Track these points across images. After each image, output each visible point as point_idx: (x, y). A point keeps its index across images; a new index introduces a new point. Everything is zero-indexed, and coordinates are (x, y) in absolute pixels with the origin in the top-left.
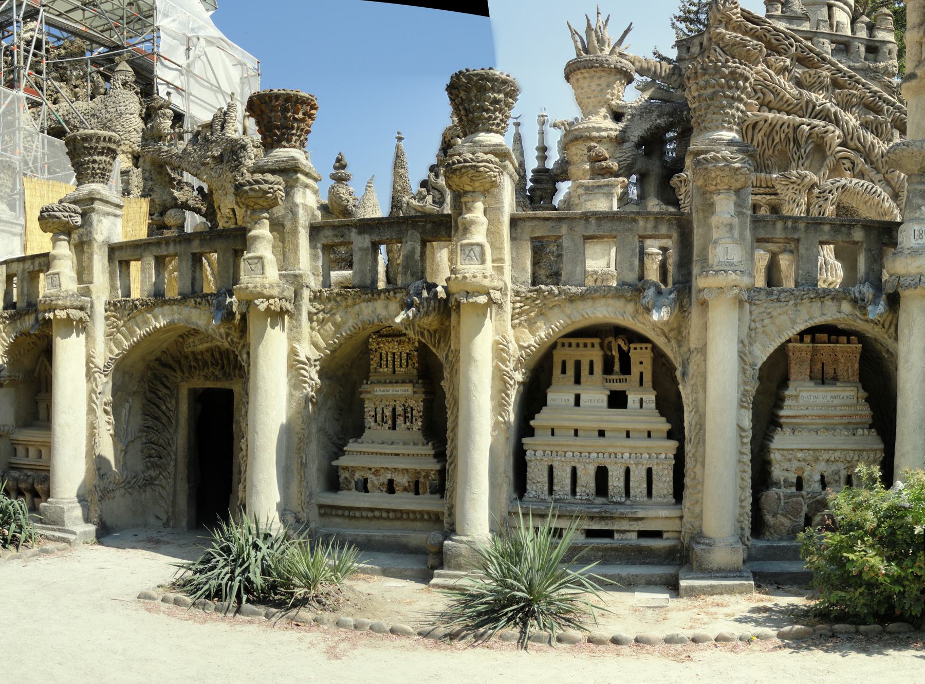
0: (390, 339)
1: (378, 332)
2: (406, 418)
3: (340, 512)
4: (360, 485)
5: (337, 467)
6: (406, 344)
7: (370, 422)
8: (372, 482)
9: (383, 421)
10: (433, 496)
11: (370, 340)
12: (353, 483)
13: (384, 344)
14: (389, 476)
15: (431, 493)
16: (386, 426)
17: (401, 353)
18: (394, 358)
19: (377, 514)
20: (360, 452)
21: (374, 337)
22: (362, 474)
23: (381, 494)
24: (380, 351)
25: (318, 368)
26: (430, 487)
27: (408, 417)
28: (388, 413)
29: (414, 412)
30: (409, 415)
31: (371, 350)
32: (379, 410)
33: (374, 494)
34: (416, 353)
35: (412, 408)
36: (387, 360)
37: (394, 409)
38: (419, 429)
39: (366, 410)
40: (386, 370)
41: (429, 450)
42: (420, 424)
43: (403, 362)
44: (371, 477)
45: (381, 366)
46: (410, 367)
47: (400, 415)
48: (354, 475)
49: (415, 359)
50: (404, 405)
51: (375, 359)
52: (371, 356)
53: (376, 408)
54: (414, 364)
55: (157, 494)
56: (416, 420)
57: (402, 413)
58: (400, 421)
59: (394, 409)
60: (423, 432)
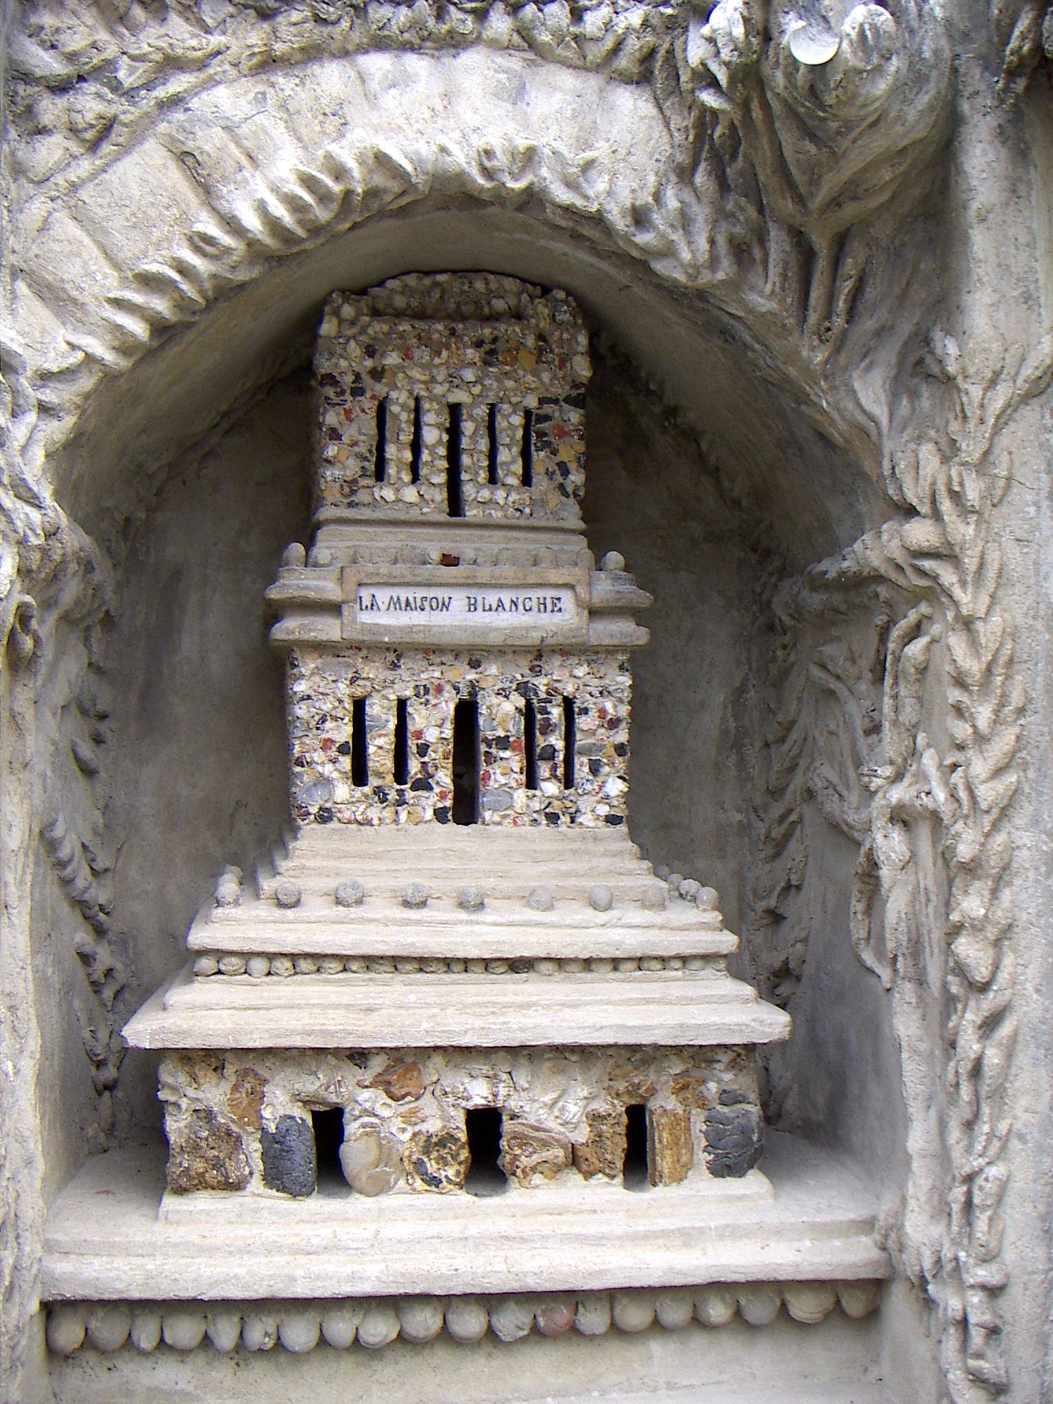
1: (363, 292)
4: (304, 1150)
5: (155, 1057)
6: (527, 360)
7: (324, 782)
8: (372, 1131)
9: (400, 774)
10: (732, 1185)
11: (328, 328)
12: (253, 1147)
13: (407, 355)
14: (479, 1093)
15: (724, 1168)
16: (429, 802)
17: (493, 411)
18: (454, 432)
20: (293, 957)
21: (348, 311)
22: (313, 1084)
23: (432, 1199)
24: (380, 389)
25: (58, 429)
27: (550, 754)
29: (582, 722)
30: (557, 741)
31: (330, 379)
32: (380, 712)
33: (389, 1201)
34: (575, 416)
35: (568, 703)
36: (416, 446)
38: (612, 820)
40: (410, 494)
42: (616, 787)
43: (503, 456)
45: (380, 474)
46: (541, 483)
47: (503, 743)
48: (257, 1097)
49: (570, 450)
50: (524, 689)
51: (350, 432)
52: (331, 418)
53: (359, 706)
54: (564, 470)
56: (595, 768)
57: (516, 728)
59: (466, 714)
60: (633, 836)
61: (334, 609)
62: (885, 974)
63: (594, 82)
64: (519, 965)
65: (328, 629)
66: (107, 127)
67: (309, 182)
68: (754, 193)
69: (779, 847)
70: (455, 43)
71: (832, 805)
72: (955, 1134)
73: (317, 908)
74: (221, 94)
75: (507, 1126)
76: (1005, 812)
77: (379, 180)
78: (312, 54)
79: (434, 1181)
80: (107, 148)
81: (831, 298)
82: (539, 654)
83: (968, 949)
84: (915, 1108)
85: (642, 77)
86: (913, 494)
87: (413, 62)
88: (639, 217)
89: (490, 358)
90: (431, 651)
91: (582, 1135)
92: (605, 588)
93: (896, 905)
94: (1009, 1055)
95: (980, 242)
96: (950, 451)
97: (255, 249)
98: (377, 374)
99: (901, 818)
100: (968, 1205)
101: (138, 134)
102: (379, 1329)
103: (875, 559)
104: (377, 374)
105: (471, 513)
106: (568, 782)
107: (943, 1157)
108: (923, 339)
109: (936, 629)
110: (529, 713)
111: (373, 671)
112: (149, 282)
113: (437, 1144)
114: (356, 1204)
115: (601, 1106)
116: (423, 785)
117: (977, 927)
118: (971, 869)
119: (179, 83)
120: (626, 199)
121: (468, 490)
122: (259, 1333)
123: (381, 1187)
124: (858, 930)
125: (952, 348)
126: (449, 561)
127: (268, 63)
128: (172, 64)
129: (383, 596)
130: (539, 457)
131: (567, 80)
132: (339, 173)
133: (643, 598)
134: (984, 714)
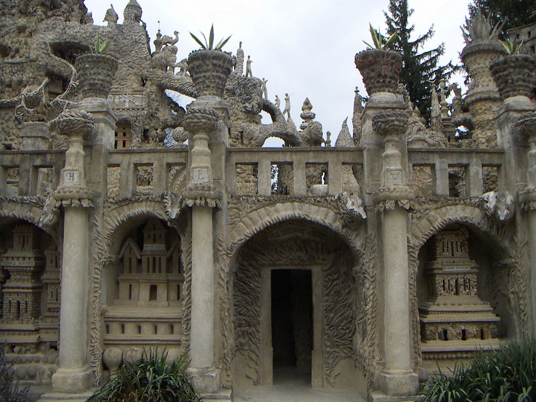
0: (450, 232)
2: (465, 287)
3: (431, 356)
7: (440, 290)
8: (451, 333)
14: (463, 328)
15: (493, 337)
16: (453, 293)
18: (452, 245)
19: (459, 355)
22: (444, 327)
23: (458, 341)
26: (492, 334)
28: (453, 283)
29: (471, 282)
31: (437, 240)
33: (453, 341)
34: (467, 242)
36: (448, 247)
37: (457, 281)
39: (437, 282)
40: (447, 254)
41: (488, 307)
42: (475, 290)
44: (450, 329)
45: (443, 251)
46: (463, 251)
47: (462, 285)
48: (438, 328)
49: (466, 247)
50: (463, 278)
51: (440, 246)
53: (444, 281)
55: (247, 357)
57: (463, 283)
58: (462, 288)
60: (478, 296)
61: (441, 269)
62: (512, 312)
63: (472, 208)
64: (467, 312)
65: (440, 272)
66: (420, 217)
67: (442, 222)
68: (492, 221)
69: (495, 298)
70: (457, 204)
71: (503, 292)
72: (522, 328)
73: (442, 306)
74: (432, 212)
75: (467, 332)
76: (525, 291)
77: (450, 221)
78: (441, 207)
79: (458, 339)
80: (420, 219)
81: (502, 232)
82: (465, 274)
83: (521, 307)
84: (517, 327)
85: (478, 206)
86: (512, 256)
87: (453, 207)
88: (479, 224)
89: (456, 236)
90: (452, 274)
91: (475, 333)
92: (473, 265)
93: (513, 303)
94: (527, 319)
95: (519, 227)
96: (516, 251)
97: (437, 230)
98: (443, 238)
99: (513, 293)
100: (524, 336)
101: (423, 217)
102: (454, 356)
103: (508, 263)
104: (443, 238)
105: (455, 256)
106: (469, 289)
107: (520, 332)
108: (512, 237)
109: (516, 271)
110: (464, 281)
111: (445, 276)
112: (426, 235)
113: (458, 334)
114: (449, 341)
115: (478, 329)
116: (452, 290)
117: (522, 304)
118: (521, 298)
119: (428, 211)
120: (477, 222)
121: (454, 253)
122: (440, 356)
123: (452, 339)
124: (508, 307)
125: (516, 239)
126: (453, 262)
127: (437, 208)
128: (427, 209)
129: (447, 267)
130: (463, 248)
131: (470, 208)
132: (446, 221)
133: (478, 266)
134: (522, 281)
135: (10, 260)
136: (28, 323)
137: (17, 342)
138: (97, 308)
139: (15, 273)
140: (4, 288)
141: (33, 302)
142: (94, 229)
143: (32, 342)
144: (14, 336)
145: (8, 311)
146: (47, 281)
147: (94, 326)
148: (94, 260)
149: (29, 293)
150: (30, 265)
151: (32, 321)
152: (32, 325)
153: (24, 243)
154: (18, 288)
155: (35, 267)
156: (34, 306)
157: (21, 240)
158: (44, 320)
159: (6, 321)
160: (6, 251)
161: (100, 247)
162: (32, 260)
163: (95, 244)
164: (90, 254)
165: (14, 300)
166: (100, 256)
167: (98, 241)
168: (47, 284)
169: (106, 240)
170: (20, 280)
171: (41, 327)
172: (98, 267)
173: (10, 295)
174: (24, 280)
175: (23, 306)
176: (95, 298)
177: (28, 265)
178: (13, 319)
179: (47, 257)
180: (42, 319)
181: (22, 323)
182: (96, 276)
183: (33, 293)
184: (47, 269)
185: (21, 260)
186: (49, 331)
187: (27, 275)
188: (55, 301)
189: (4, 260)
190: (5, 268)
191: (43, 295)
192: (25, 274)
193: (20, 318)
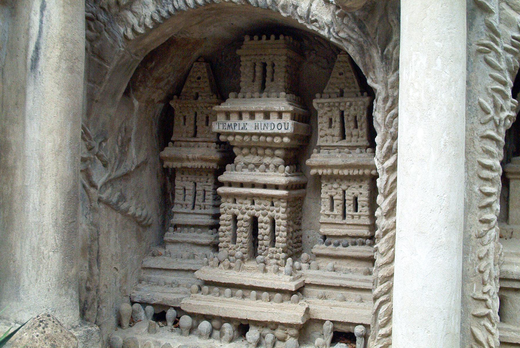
135: (234, 118)
136: (278, 271)
137: (254, 317)
138: (491, 257)
139: (245, 151)
140: (222, 184)
141: (288, 219)
142: (480, 20)
143: (289, 321)
144: (247, 300)
145: (229, 239)
146: (320, 172)
147: (482, 311)
148: (480, 113)
149: (279, 198)
150: (283, 131)
151: (288, 268)
152: (288, 278)
153: (264, 81)
154: (253, 185)
155: (292, 137)
156: (291, 230)
157: (259, 74)
158: (313, 263)
159: (227, 262)
160: (223, 99)
161: (497, 74)
162: (287, 119)
163: (483, 65)
164: (469, 94)
165: (244, 213)
166: (500, 101)
167: (491, 57)
168: (318, 178)
169: (509, 56)
170: (257, 166)
171: (308, 280)
172: (493, 133)
173: (235, 201)
174: (267, 166)
175: (264, 230)
176: (485, 227)
177: (276, 130)
178: (243, 259)
179: (320, 113)
180: (308, 262)
181: (265, 271)
182: (488, 161)
183: (287, 199)
184: (320, 142)
185: (259, 118)
186: (328, 291)
187: (273, 156)
188: (339, 220)
189: (221, 118)
190: (222, 138)
191: (309, 202)
192: (268, 151)
193: (259, 258)
